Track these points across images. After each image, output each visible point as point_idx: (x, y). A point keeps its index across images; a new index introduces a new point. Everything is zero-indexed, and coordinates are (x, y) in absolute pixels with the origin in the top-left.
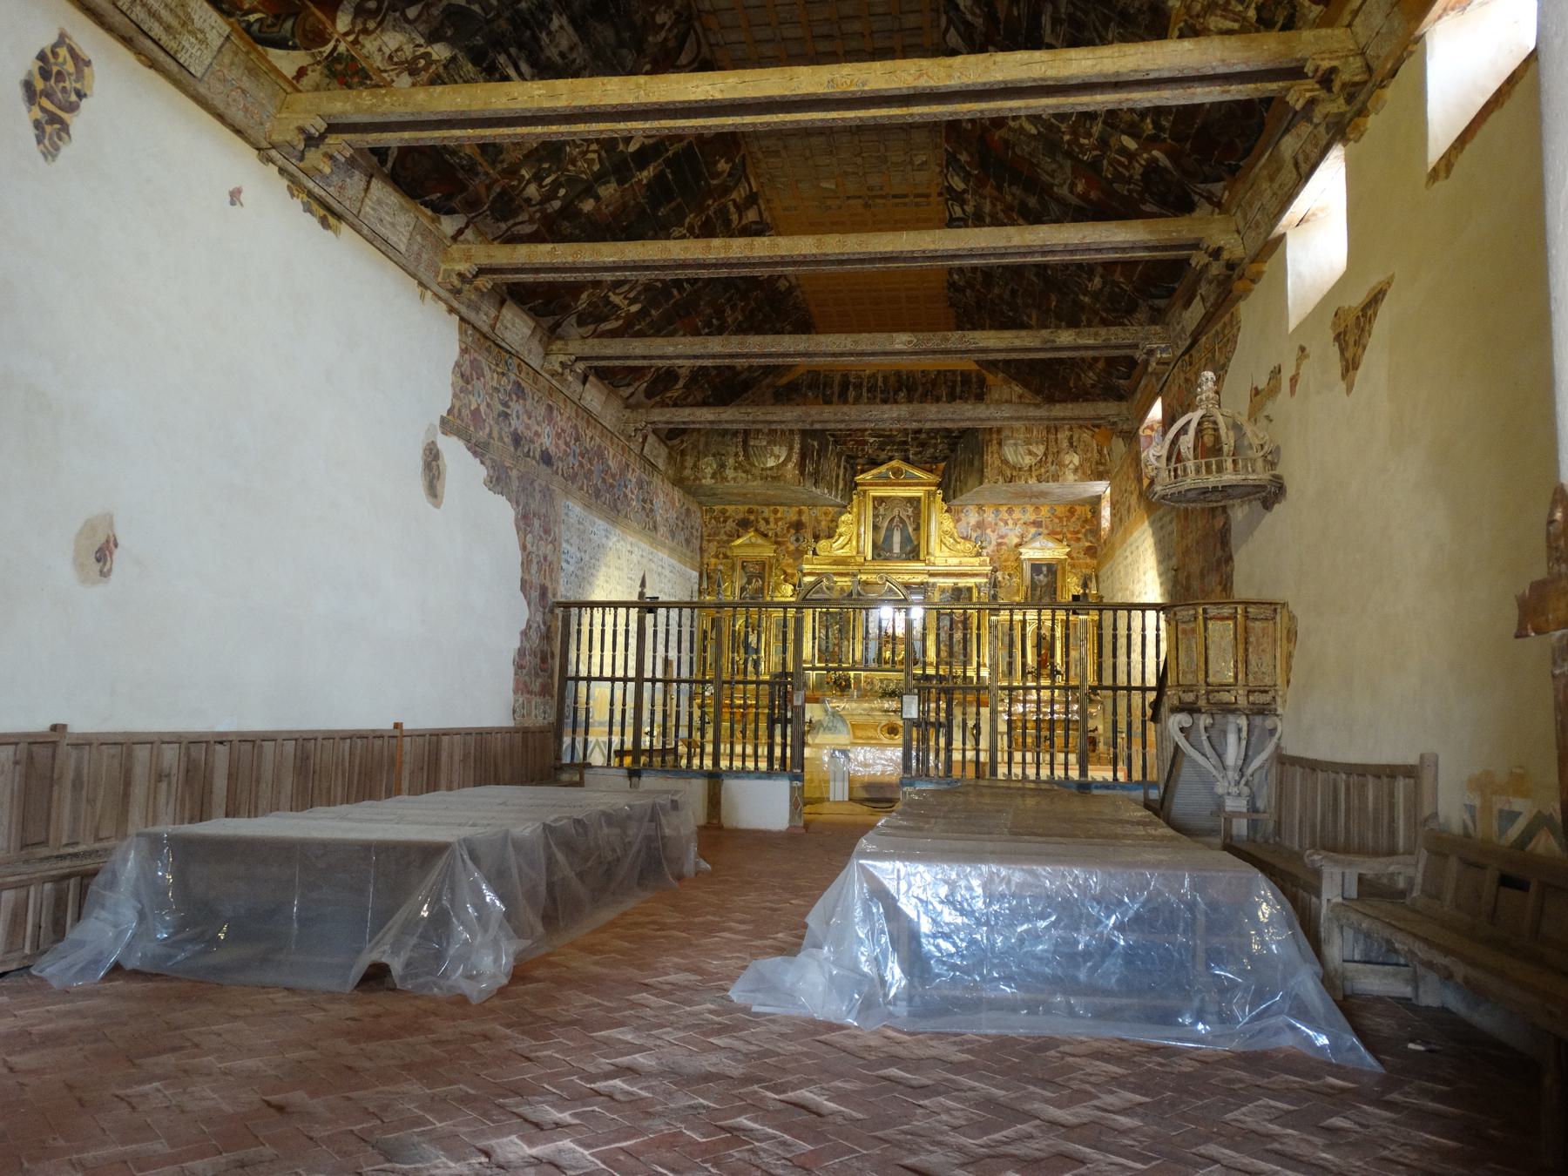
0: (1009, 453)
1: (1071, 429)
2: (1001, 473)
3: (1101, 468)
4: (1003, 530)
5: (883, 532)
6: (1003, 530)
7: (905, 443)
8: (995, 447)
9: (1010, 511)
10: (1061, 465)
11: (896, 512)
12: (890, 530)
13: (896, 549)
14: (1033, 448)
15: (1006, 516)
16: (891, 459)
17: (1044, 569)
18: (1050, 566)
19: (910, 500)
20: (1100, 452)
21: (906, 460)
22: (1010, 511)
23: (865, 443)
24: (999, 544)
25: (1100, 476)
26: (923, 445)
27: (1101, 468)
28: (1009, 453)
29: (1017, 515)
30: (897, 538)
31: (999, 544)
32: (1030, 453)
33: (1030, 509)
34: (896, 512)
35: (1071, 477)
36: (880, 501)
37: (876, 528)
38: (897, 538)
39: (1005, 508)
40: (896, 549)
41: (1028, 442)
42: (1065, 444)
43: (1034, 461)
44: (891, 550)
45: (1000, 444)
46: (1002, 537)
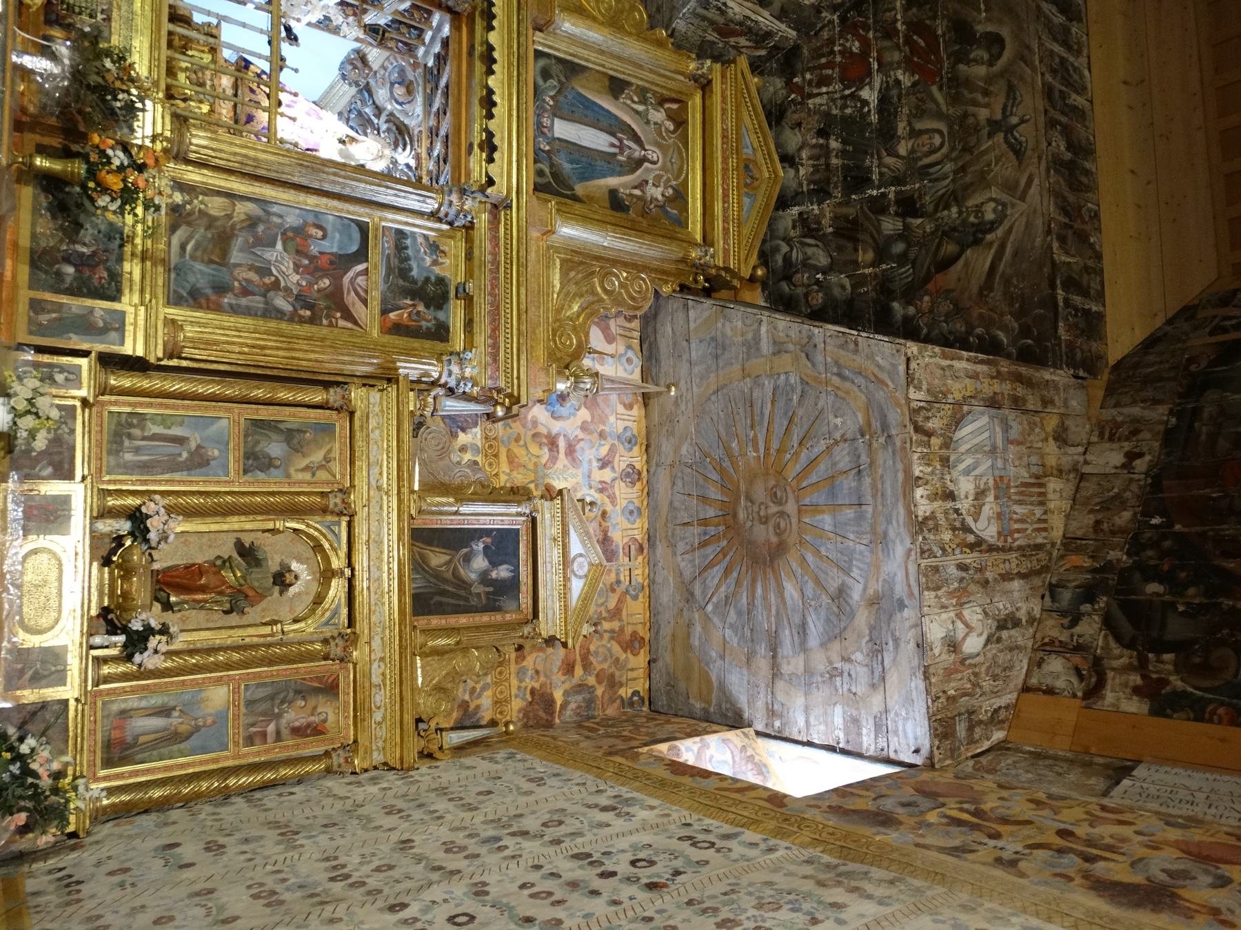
0: (977, 430)
1: (1032, 620)
2: (937, 397)
3: (961, 730)
4: (589, 454)
5: (606, 103)
6: (589, 454)
7: (857, 179)
8: (989, 388)
9: (632, 476)
10: (961, 597)
11: (653, 153)
12: (613, 126)
13: (563, 129)
14: (990, 507)
15: (621, 463)
16: (788, 160)
17: (503, 572)
18: (512, 586)
19: (679, 197)
20: (995, 719)
21: (783, 203)
22: (632, 476)
23: (863, 78)
24: (552, 442)
25: (942, 728)
26: (848, 231)
27: (961, 730)
28: (977, 430)
29: (627, 494)
30: (594, 139)
31: (552, 442)
32: (980, 494)
33: (638, 529)
34: (653, 153)
35: (936, 631)
36: (680, 123)
37: (616, 87)
38: (594, 139)
39: (639, 463)
40: (563, 129)
41: (1001, 487)
42: (1002, 606)
43: (964, 505)
44: (557, 113)
45: (993, 403)
46: (571, 451)
